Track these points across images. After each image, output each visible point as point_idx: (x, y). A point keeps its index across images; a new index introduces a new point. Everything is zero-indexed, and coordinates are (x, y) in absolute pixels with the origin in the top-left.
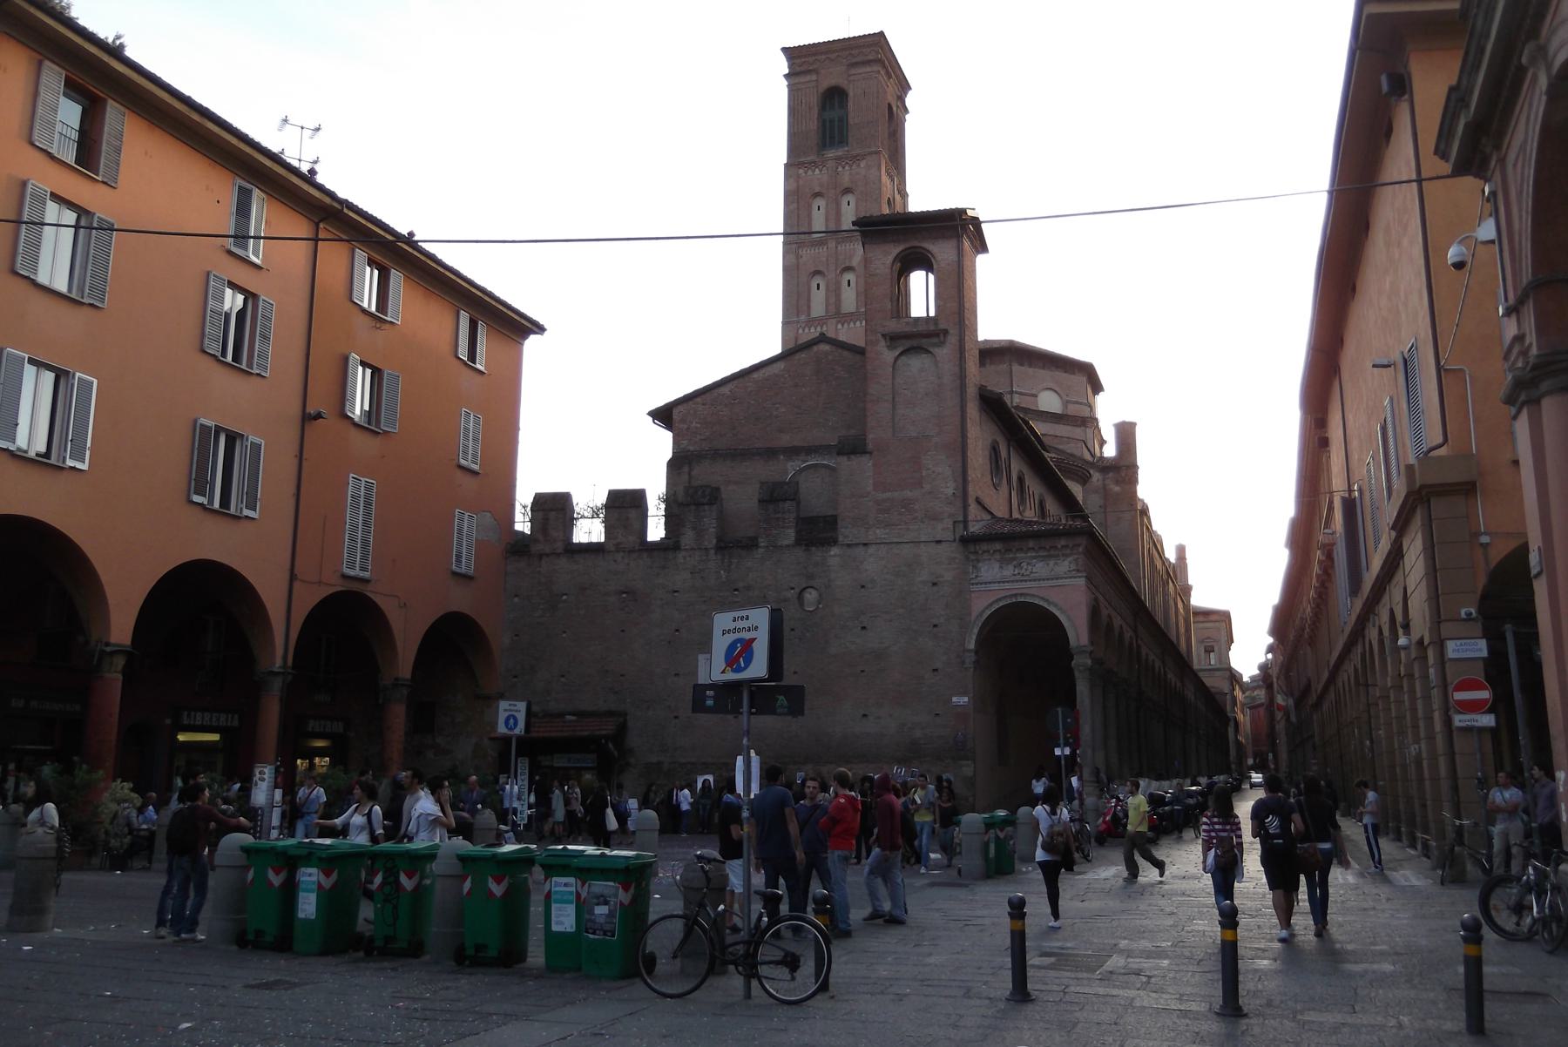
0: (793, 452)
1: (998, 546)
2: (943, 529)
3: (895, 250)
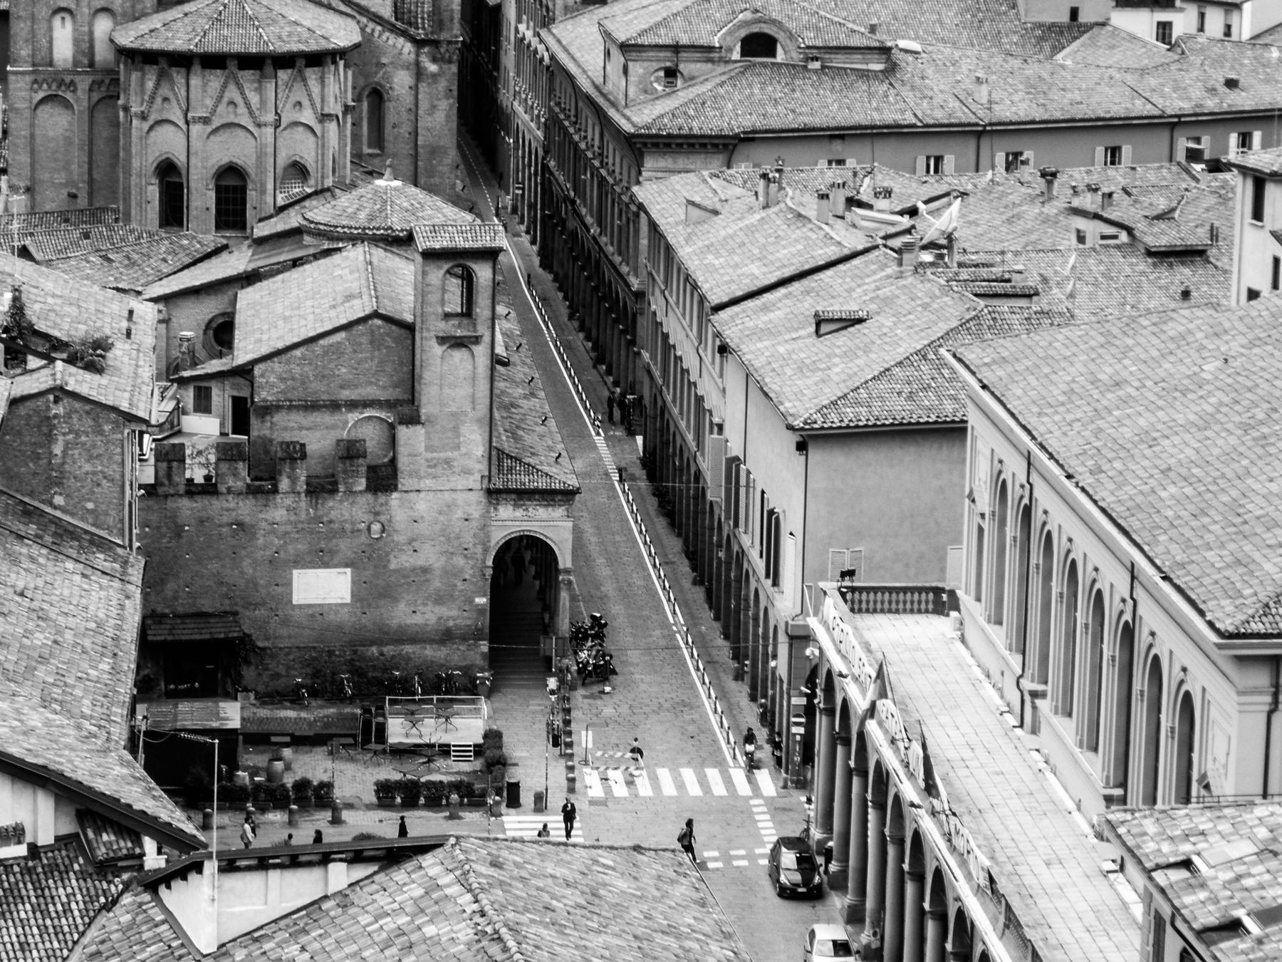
0: (353, 405)
1: (513, 496)
2: (474, 481)
3: (446, 266)
